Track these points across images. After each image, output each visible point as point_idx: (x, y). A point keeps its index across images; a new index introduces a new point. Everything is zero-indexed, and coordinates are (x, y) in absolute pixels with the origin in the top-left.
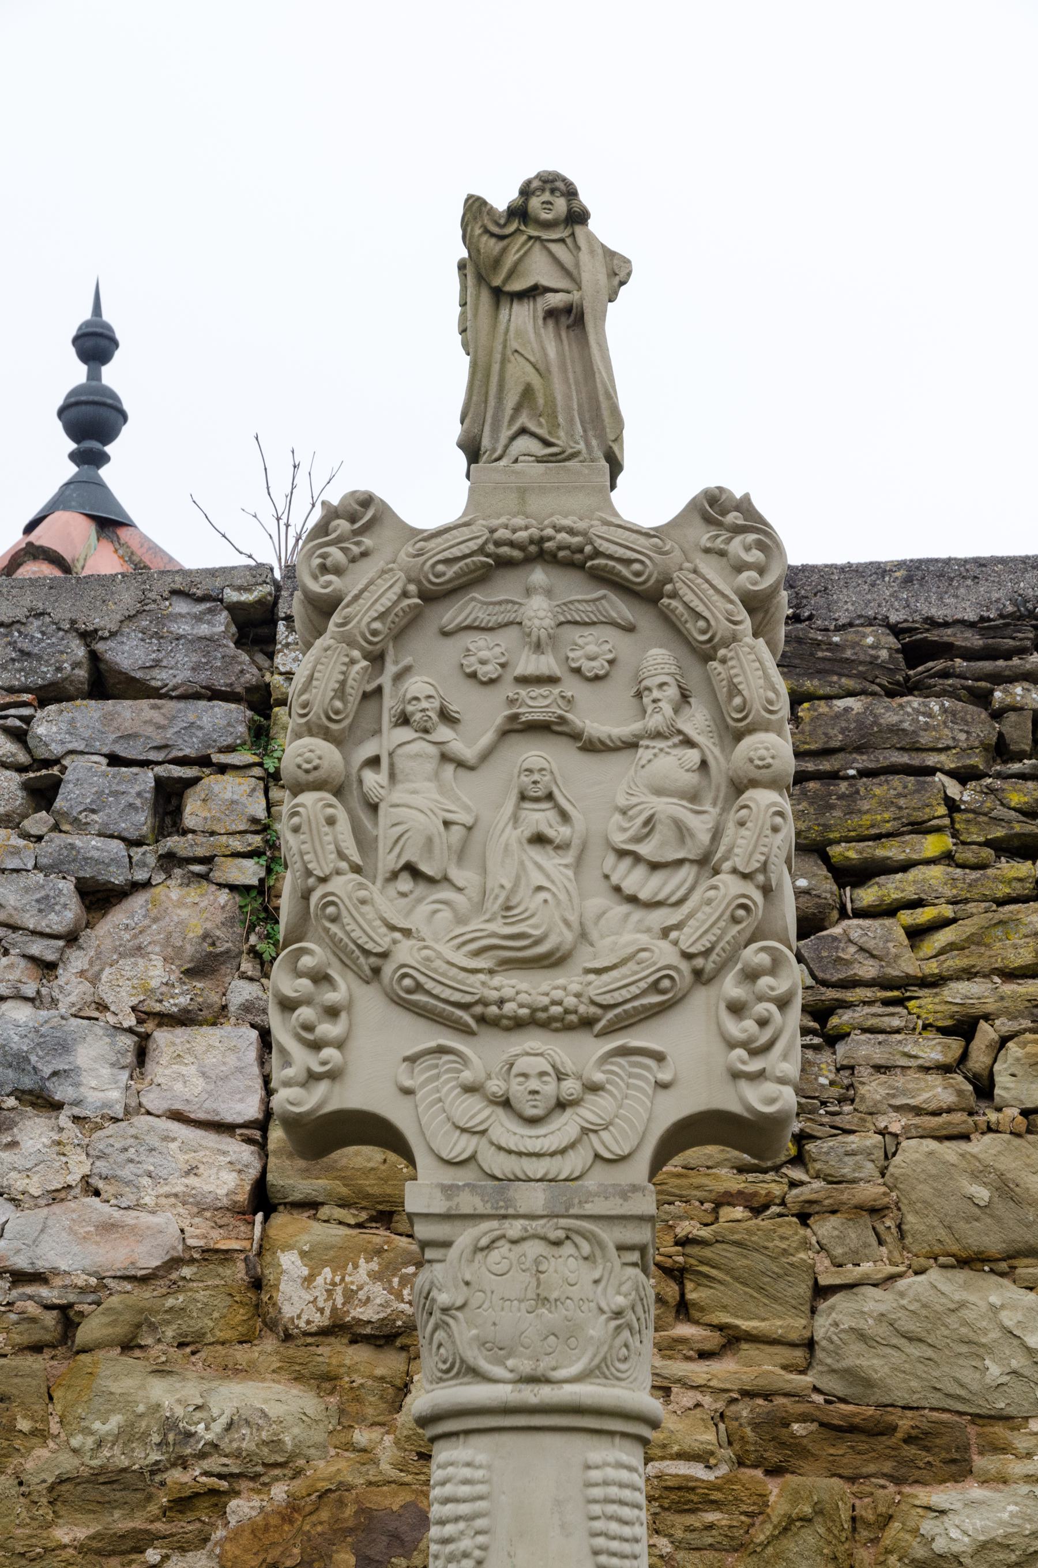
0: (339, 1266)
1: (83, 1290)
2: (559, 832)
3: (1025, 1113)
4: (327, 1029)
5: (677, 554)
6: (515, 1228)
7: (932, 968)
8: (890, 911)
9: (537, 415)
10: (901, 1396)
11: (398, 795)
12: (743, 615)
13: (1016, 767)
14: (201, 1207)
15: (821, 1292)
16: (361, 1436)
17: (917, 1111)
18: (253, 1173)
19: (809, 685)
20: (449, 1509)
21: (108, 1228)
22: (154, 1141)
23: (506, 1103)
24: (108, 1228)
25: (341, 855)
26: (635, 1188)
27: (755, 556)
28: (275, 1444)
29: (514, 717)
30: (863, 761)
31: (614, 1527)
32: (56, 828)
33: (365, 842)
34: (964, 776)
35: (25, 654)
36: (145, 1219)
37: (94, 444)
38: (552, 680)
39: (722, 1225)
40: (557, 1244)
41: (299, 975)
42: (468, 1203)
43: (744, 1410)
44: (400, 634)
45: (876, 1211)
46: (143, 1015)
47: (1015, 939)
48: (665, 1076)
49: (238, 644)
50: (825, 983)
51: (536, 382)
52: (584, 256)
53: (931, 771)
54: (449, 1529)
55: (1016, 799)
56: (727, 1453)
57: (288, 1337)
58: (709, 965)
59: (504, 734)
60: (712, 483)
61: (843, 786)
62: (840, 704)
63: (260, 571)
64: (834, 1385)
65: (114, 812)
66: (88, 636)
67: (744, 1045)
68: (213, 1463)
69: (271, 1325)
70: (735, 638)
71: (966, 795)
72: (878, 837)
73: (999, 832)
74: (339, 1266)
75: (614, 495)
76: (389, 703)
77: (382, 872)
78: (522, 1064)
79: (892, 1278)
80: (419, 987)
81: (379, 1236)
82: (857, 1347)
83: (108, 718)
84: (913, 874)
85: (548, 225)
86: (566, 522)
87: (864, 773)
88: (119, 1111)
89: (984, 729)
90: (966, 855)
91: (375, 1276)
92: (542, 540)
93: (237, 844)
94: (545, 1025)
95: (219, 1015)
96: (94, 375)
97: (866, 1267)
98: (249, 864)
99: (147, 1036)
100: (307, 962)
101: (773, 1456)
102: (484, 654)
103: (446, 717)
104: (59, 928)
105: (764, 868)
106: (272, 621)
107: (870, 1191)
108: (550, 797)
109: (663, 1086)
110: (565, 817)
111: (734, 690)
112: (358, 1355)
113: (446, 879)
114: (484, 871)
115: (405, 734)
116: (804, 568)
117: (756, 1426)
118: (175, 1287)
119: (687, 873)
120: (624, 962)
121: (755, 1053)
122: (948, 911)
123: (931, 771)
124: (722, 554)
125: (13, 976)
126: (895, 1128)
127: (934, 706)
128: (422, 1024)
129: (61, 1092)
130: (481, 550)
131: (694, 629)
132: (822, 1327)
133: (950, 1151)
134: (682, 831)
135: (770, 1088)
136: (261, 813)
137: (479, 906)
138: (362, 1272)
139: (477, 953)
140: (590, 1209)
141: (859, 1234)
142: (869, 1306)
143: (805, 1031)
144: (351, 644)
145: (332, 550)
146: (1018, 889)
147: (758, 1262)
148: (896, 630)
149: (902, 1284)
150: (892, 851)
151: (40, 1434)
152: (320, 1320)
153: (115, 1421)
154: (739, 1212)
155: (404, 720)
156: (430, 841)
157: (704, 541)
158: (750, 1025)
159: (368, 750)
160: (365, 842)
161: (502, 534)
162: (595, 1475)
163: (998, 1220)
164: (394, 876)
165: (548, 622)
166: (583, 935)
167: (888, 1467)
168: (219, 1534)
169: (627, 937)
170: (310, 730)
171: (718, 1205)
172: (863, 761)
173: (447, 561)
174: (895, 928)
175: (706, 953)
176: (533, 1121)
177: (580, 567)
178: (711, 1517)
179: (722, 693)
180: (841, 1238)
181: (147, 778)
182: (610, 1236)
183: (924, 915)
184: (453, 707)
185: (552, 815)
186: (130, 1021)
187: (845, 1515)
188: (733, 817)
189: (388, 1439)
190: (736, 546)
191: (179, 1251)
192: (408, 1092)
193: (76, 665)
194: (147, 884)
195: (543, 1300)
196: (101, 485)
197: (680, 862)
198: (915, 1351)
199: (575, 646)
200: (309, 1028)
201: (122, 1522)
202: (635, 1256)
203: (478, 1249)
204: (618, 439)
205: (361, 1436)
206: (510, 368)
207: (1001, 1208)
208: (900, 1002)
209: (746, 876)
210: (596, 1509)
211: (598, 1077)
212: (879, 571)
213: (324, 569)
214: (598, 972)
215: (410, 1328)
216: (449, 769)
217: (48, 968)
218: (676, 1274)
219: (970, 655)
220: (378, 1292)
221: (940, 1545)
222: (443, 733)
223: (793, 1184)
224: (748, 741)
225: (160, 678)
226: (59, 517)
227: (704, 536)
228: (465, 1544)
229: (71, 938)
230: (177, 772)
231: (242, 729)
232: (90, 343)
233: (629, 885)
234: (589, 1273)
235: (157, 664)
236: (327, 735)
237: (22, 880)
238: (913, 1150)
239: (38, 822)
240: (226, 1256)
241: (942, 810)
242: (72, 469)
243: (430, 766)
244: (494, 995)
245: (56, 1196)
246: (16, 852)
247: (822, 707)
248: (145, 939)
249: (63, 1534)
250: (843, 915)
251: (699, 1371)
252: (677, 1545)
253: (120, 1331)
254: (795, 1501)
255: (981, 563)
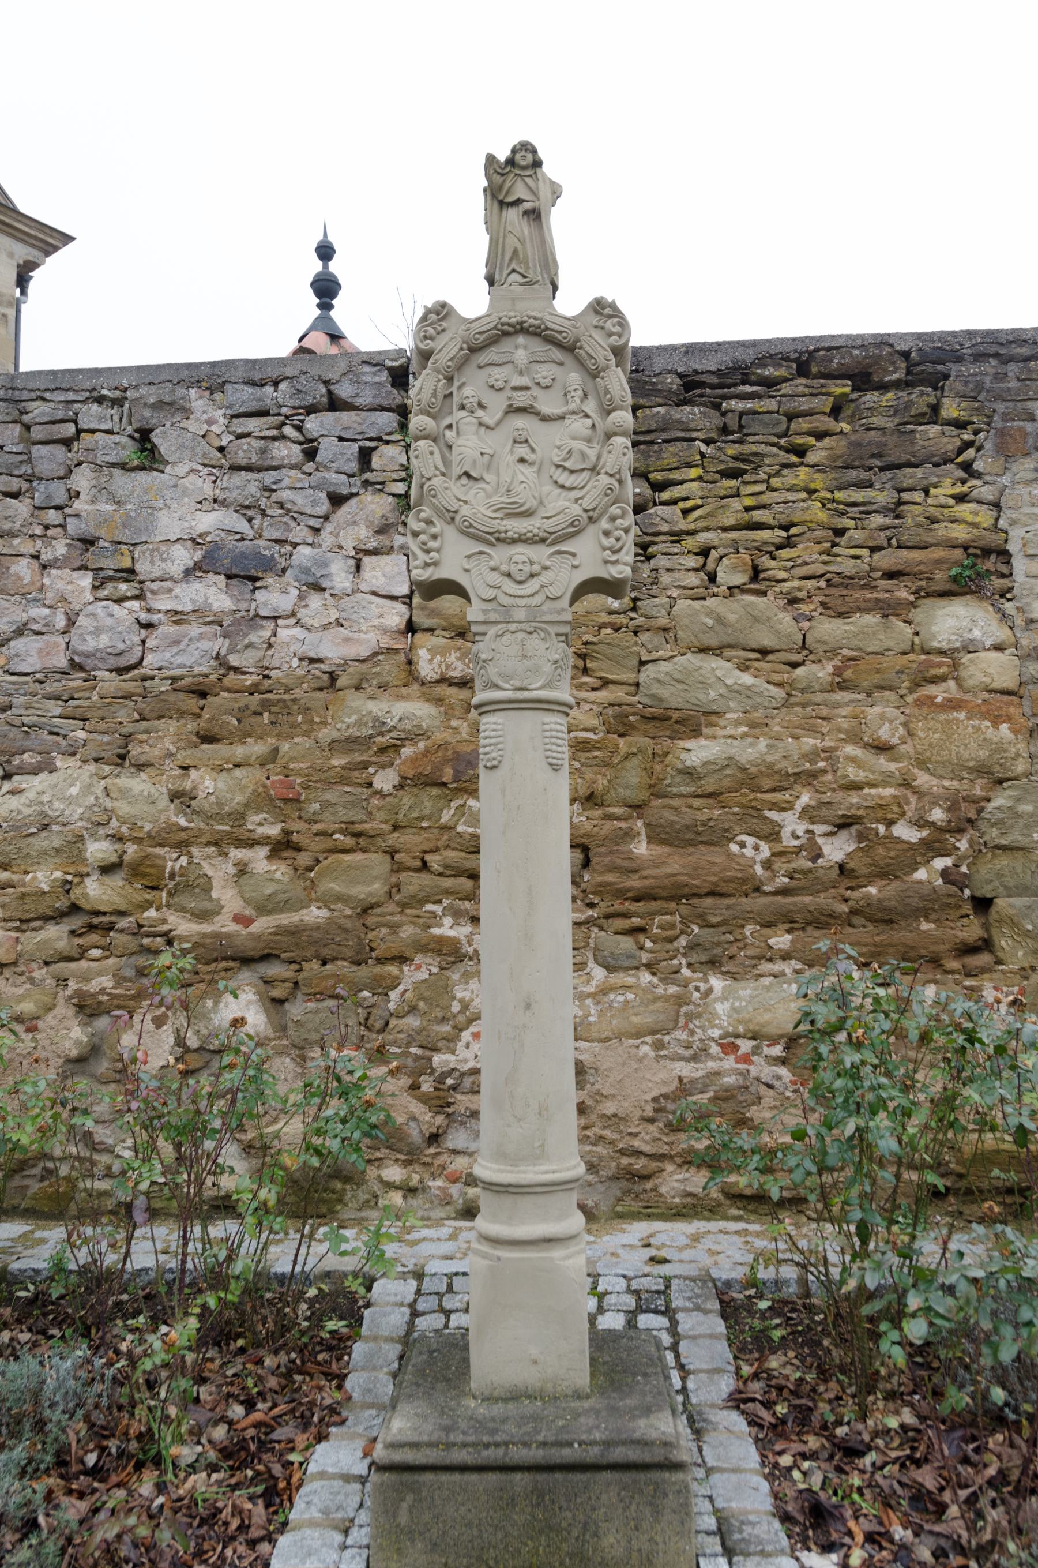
0: (443, 655)
1: (338, 665)
2: (530, 457)
3: (729, 588)
4: (432, 544)
5: (582, 328)
6: (513, 627)
7: (692, 527)
8: (674, 502)
9: (520, 263)
10: (674, 705)
11: (460, 442)
12: (612, 357)
13: (731, 438)
14: (385, 631)
15: (642, 663)
16: (454, 723)
17: (684, 588)
18: (407, 616)
19: (642, 401)
20: (487, 741)
21: (347, 640)
22: (365, 604)
23: (509, 575)
24: (347, 640)
25: (436, 468)
26: (563, 610)
27: (617, 329)
28: (419, 726)
29: (511, 406)
30: (665, 436)
31: (554, 747)
32: (317, 469)
33: (446, 462)
34: (708, 442)
35: (299, 391)
36: (363, 636)
37: (327, 300)
38: (527, 388)
39: (602, 636)
40: (530, 633)
41: (420, 521)
42: (493, 617)
43: (610, 711)
44: (459, 368)
45: (665, 630)
46: (358, 551)
47: (728, 514)
48: (576, 563)
49: (393, 386)
50: (646, 534)
51: (519, 246)
52: (541, 183)
53: (694, 440)
54: (487, 749)
55: (730, 452)
56: (603, 728)
57: (423, 684)
58: (595, 514)
59: (507, 413)
60: (598, 295)
61: (656, 447)
62: (655, 410)
63: (401, 352)
64: (647, 701)
65: (342, 462)
66: (326, 383)
67: (610, 549)
68: (394, 734)
69: (416, 679)
70: (608, 367)
71: (708, 450)
72: (670, 470)
73: (722, 467)
74: (443, 655)
75: (555, 302)
76: (456, 399)
77: (455, 476)
78: (515, 558)
79: (672, 657)
80: (471, 526)
81: (459, 642)
82: (657, 685)
83: (337, 420)
84: (685, 486)
85: (524, 168)
86: (533, 314)
87: (665, 441)
88: (349, 591)
89: (717, 420)
90: (708, 477)
91: (458, 659)
92: (522, 323)
93: (395, 476)
94: (525, 541)
95: (390, 550)
96: (325, 267)
97: (661, 653)
98: (400, 484)
99: (359, 560)
100: (423, 515)
101: (622, 729)
102: (497, 376)
103: (481, 406)
104: (320, 514)
105: (619, 472)
106: (406, 375)
107: (663, 621)
108: (526, 441)
109: (575, 567)
110: (533, 450)
111: (607, 391)
112: (452, 691)
113: (482, 478)
114: (498, 475)
115: (463, 413)
116: (641, 348)
117: (615, 717)
118: (376, 664)
119: (586, 475)
120: (558, 514)
121: (614, 552)
122: (699, 502)
123: (694, 440)
124: (602, 328)
125: (303, 534)
126: (675, 595)
127: (696, 410)
128: (473, 542)
129: (325, 584)
130: (495, 328)
131: (590, 364)
132: (642, 678)
133: (697, 604)
134: (584, 456)
135: (620, 567)
136: (405, 462)
137: (497, 490)
138: (453, 656)
139: (496, 511)
140: (544, 619)
141: (658, 639)
142: (662, 669)
143: (637, 555)
144: (439, 372)
145: (429, 328)
146: (730, 492)
147: (617, 651)
148: (680, 376)
149: (675, 659)
150: (676, 476)
151: (324, 723)
152: (436, 677)
153: (354, 718)
154: (609, 631)
155: (463, 407)
156: (475, 461)
157: (595, 322)
158: (612, 540)
159: (447, 421)
160: (446, 462)
161: (505, 320)
162: (547, 727)
163: (716, 633)
164: (460, 477)
165: (525, 361)
166: (541, 503)
167: (668, 733)
168: (398, 762)
169: (560, 503)
170: (422, 412)
171: (600, 628)
172: (665, 436)
173: (480, 333)
174: (677, 509)
175: (594, 509)
176: (520, 582)
177: (539, 335)
178: (596, 753)
179: (602, 394)
180: (651, 641)
181: (355, 447)
182: (553, 630)
183: (689, 504)
184: (484, 401)
185: (527, 449)
186: (353, 553)
187: (650, 752)
188: (606, 449)
189: (465, 724)
190: (609, 324)
191: (377, 649)
192: (467, 571)
193: (322, 396)
194: (357, 494)
195: (525, 657)
196: (331, 319)
197: (583, 470)
198: (680, 686)
199: (538, 373)
200: (424, 544)
201: (358, 757)
202: (563, 638)
203: (497, 636)
204: (556, 274)
205: (454, 723)
206: (507, 240)
207: (718, 628)
208: (678, 542)
209: (611, 475)
210: (547, 740)
211: (548, 563)
212: (673, 348)
213: (426, 338)
214: (548, 518)
215: (472, 680)
216: (483, 429)
217: (317, 531)
218: (583, 656)
219: (713, 387)
220: (460, 665)
221: (688, 763)
222: (480, 413)
223: (632, 619)
224: (613, 415)
225: (359, 401)
226: (313, 334)
227: (595, 320)
228: (494, 755)
229: (326, 518)
230: (368, 444)
231: (395, 424)
232: (323, 250)
233: (561, 481)
234: (543, 646)
235: (357, 395)
236: (429, 414)
237: (304, 493)
238: (682, 605)
239: (309, 467)
240: (396, 651)
241: (698, 457)
242: (318, 312)
243: (474, 428)
244: (503, 529)
245: (325, 627)
246: (300, 480)
247: (648, 411)
248: (357, 518)
249: (335, 762)
250: (655, 504)
251: (592, 696)
252: (582, 764)
253: (354, 682)
254: (630, 747)
255: (719, 344)
